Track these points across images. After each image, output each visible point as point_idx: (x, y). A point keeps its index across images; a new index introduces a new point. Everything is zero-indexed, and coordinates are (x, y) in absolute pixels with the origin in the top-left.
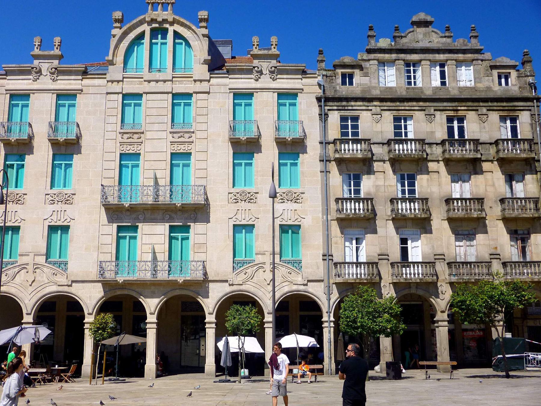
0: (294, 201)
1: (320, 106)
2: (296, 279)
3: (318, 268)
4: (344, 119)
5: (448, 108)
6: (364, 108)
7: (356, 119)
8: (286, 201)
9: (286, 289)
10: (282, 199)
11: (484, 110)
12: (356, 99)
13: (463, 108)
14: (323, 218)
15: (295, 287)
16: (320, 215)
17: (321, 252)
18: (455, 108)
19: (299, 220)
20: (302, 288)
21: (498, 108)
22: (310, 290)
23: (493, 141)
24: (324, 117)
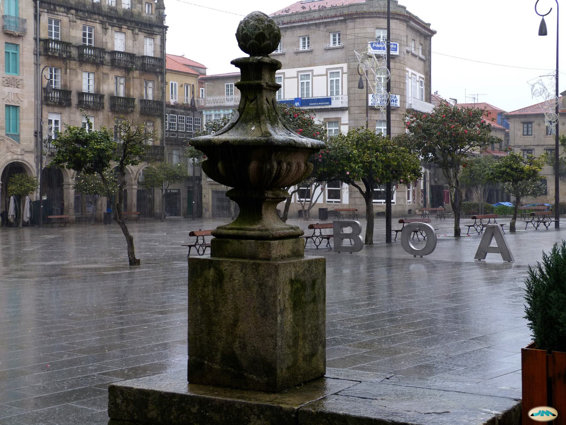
0: (16, 86)
1: (36, 8)
2: (16, 150)
3: (31, 142)
4: (50, 21)
5: (117, 25)
6: (65, 14)
7: (57, 22)
8: (11, 85)
9: (9, 158)
10: (8, 83)
11: (137, 31)
12: (60, 6)
13: (125, 27)
14: (35, 102)
15: (15, 157)
16: (33, 100)
17: (32, 130)
18: (120, 26)
19: (19, 102)
20: (20, 157)
21: (145, 31)
22: (26, 159)
23: (140, 56)
24: (37, 17)
